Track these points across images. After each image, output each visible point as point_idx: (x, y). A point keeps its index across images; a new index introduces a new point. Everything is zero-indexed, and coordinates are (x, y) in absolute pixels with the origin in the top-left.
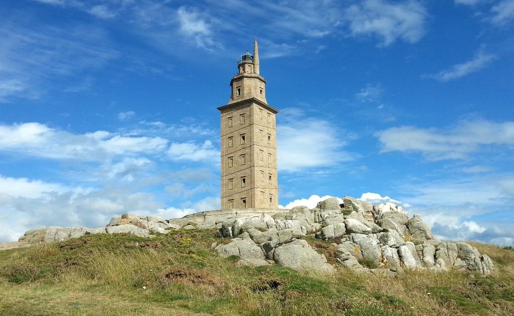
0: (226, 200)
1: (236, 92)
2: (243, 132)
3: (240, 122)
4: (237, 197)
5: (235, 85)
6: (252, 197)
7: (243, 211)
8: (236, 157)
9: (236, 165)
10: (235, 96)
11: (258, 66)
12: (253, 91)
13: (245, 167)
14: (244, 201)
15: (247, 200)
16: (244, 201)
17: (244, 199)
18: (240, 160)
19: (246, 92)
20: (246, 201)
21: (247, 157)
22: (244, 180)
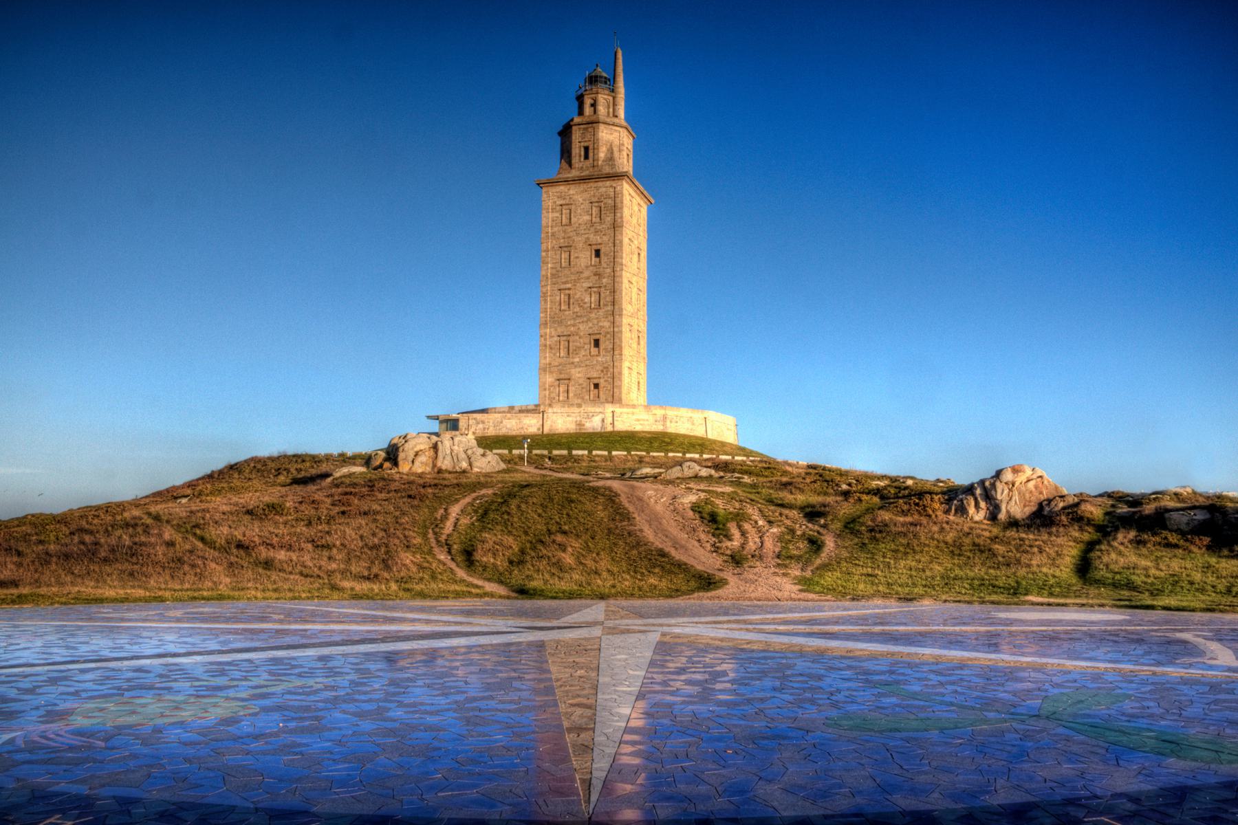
0: (549, 379)
1: (577, 150)
2: (594, 239)
3: (588, 218)
4: (577, 374)
5: (576, 135)
6: (615, 379)
7: (625, 410)
8: (579, 293)
9: (577, 309)
10: (575, 160)
11: (623, 103)
12: (616, 154)
13: (601, 313)
14: (596, 386)
15: (602, 383)
16: (596, 386)
17: (596, 381)
18: (587, 299)
19: (602, 155)
20: (601, 385)
21: (606, 294)
22: (597, 343)
